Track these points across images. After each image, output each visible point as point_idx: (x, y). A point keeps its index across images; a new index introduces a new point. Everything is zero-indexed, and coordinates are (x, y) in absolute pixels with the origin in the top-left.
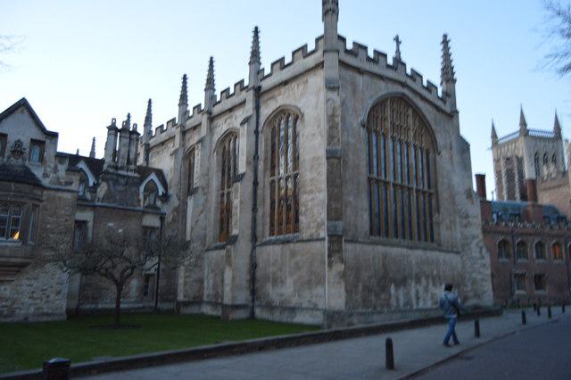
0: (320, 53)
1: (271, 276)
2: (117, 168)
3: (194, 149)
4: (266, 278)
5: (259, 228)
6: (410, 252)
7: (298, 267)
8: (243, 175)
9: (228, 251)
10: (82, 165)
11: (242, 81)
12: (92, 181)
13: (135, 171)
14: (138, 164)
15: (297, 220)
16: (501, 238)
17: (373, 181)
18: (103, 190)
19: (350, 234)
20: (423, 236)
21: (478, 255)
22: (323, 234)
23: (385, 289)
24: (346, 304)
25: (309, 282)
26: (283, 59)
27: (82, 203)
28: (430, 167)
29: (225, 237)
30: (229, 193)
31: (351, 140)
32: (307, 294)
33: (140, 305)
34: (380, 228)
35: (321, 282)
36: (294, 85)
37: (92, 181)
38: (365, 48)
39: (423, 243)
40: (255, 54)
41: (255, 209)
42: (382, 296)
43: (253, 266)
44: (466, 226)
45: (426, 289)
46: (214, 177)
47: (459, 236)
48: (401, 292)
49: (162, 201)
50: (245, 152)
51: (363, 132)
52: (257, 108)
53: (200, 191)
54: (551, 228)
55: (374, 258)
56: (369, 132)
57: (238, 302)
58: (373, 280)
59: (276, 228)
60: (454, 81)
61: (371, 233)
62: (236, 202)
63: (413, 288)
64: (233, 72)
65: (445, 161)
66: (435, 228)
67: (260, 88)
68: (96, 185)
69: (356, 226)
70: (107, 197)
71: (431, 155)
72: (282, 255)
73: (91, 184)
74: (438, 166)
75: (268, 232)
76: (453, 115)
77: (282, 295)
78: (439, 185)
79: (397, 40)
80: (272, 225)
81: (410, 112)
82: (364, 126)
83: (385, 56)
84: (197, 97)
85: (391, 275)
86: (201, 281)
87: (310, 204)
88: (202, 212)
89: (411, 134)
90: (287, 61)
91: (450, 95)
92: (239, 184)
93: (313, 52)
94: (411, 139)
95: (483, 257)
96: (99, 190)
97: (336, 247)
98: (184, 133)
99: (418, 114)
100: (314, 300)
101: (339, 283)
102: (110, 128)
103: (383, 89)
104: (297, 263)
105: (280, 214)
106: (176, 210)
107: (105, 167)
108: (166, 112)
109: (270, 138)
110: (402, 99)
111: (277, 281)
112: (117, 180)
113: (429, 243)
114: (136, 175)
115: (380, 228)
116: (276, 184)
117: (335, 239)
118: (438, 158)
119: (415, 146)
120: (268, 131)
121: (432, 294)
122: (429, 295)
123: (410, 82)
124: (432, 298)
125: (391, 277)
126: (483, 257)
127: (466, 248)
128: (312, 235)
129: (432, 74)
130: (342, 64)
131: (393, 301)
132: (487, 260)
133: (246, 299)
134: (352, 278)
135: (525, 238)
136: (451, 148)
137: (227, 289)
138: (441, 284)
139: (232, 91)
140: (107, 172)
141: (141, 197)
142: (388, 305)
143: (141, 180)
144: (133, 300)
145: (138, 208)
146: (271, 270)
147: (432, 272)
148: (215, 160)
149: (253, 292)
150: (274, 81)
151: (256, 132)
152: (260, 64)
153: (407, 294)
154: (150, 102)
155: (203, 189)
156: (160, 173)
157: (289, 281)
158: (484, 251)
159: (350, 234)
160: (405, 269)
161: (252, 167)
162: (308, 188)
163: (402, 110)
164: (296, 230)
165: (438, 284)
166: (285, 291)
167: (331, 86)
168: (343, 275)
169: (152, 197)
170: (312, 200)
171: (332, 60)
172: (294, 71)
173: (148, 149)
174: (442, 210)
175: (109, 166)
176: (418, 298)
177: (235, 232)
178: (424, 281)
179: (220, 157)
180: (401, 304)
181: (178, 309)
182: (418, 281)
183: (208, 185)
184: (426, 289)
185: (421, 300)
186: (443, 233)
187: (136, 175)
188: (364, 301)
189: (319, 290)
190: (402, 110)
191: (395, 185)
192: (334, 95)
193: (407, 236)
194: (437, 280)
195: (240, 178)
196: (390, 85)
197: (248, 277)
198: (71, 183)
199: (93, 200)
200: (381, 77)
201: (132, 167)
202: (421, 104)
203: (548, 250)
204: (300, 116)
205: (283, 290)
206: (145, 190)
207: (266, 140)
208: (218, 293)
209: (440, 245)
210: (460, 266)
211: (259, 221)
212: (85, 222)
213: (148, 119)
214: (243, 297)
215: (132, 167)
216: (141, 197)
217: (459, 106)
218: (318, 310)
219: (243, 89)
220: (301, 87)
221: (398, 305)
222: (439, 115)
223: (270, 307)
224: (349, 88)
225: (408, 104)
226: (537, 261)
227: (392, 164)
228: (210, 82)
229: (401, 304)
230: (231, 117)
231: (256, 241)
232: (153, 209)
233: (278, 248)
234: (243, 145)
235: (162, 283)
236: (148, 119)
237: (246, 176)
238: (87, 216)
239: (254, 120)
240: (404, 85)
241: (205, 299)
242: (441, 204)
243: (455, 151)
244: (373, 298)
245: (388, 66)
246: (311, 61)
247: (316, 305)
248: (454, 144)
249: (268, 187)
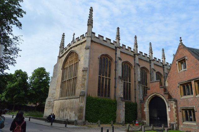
6: (66, 100)
138: (73, 111)
176: (66, 116)
178: (68, 110)
184: (68, 112)
185: (67, 116)
194: (72, 109)
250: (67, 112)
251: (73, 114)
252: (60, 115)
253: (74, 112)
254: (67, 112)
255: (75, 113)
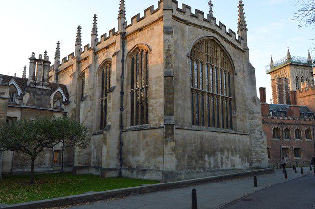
0: (161, 11)
1: (131, 150)
2: (35, 84)
3: (84, 72)
4: (128, 152)
5: (124, 121)
6: (217, 135)
7: (147, 145)
8: (114, 88)
9: (105, 135)
10: (12, 82)
11: (114, 29)
12: (19, 92)
13: (48, 86)
14: (50, 82)
15: (147, 115)
16: (275, 126)
17: (195, 91)
18: (26, 97)
19: (180, 124)
20: (225, 125)
21: (260, 137)
22: (162, 124)
23: (201, 157)
24: (177, 166)
25: (154, 154)
26: (138, 15)
27: (11, 106)
28: (231, 83)
29: (103, 126)
30: (106, 99)
31: (180, 65)
32: (153, 161)
33: (52, 169)
34: (198, 120)
35: (162, 153)
36: (145, 31)
37: (19, 92)
38: (190, 8)
39: (226, 130)
40: (122, 13)
41: (121, 109)
42: (200, 162)
43: (121, 144)
44: (252, 119)
45: (228, 158)
46: (97, 90)
47: (248, 125)
48: (212, 160)
49: (65, 105)
50: (115, 74)
51: (188, 60)
52: (123, 46)
53: (88, 98)
54: (305, 120)
55: (195, 138)
56: (191, 59)
57: (111, 167)
58: (194, 152)
59: (135, 120)
60: (246, 30)
61: (193, 123)
62: (109, 105)
63: (219, 156)
64: (108, 24)
65: (240, 79)
66: (233, 119)
67: (124, 33)
68: (22, 95)
69: (183, 119)
70: (29, 102)
71: (231, 76)
72: (138, 136)
73: (19, 94)
74: (235, 82)
75: (130, 123)
76: (245, 51)
77: (138, 162)
78: (236, 94)
79: (210, 4)
80: (132, 118)
81: (218, 49)
82: (188, 57)
83: (202, 13)
84: (86, 40)
85: (206, 149)
86: (89, 154)
87: (155, 105)
88: (89, 112)
89: (219, 62)
90: (141, 16)
91: (243, 38)
92: (111, 93)
93: (157, 10)
94: (219, 66)
95: (263, 138)
96: (24, 98)
97: (170, 132)
98: (79, 62)
99: (223, 49)
100: (157, 164)
101: (172, 154)
102: (31, 59)
103: (202, 34)
104: (147, 142)
105: (137, 112)
106: (74, 110)
107: (28, 83)
108: (68, 49)
109: (131, 65)
110: (213, 41)
111: (135, 153)
112: (36, 92)
113: (230, 130)
114: (48, 88)
115: (198, 120)
116: (135, 93)
117: (169, 128)
118: (235, 77)
119: (221, 70)
120: (129, 61)
121: (231, 160)
122: (230, 161)
123: (218, 30)
124: (231, 163)
125: (204, 150)
126: (263, 138)
127: (252, 132)
128: (156, 125)
129: (232, 25)
130: (175, 17)
131: (207, 165)
132: (265, 140)
133: (116, 165)
134: (180, 151)
135: (289, 126)
136: (244, 71)
137: (104, 158)
139: (108, 36)
140: (29, 87)
141: (52, 102)
142: (204, 168)
143: (51, 92)
144: (46, 166)
145: (50, 109)
146: (131, 146)
147: (231, 147)
148: (98, 80)
149: (121, 160)
150: (133, 29)
151: (122, 61)
152: (125, 18)
153: (215, 161)
154: (58, 43)
155: (90, 97)
156: (64, 88)
157: (142, 153)
158: (263, 133)
159: (180, 124)
160: (214, 146)
161: (119, 83)
162: (154, 96)
163: (213, 47)
164: (147, 122)
165: (235, 155)
166: (140, 159)
167: (168, 31)
168: (174, 149)
169: (59, 103)
170: (156, 103)
171: (169, 14)
172: (143, 23)
173: (57, 73)
174: (237, 109)
175: (31, 83)
176: (222, 163)
177: (109, 123)
178: (226, 153)
179: (101, 77)
180: (212, 166)
181: (75, 171)
182: (222, 152)
183: (93, 94)
184: (228, 158)
186: (238, 123)
187: (48, 88)
188: (188, 164)
189: (160, 159)
190: (213, 47)
191: (208, 94)
192: (168, 37)
193: (216, 124)
194: (234, 152)
195: (112, 90)
196: (205, 32)
197: (117, 151)
198: (4, 93)
199: (20, 105)
200: (200, 27)
201: (46, 83)
202: (225, 44)
203: (303, 134)
204: (149, 51)
205: (138, 159)
206: (54, 98)
207: (129, 66)
208: (99, 161)
209: (236, 130)
210: (248, 143)
211: (124, 117)
212: (16, 118)
213: (57, 54)
214: (114, 163)
215: (46, 83)
216: (52, 102)
217: (248, 46)
218: (160, 171)
219: (115, 34)
220: (149, 33)
221: (210, 168)
222: (236, 51)
223: (131, 169)
224: (180, 34)
225: (218, 44)
226: (296, 140)
227: (207, 80)
228: (95, 30)
229: (212, 166)
230: (107, 52)
231: (122, 128)
232: (59, 110)
233: (135, 133)
234: (114, 68)
235: (66, 155)
236: (57, 54)
237: (116, 89)
238: (16, 114)
239: (121, 53)
240: (214, 32)
241: (92, 165)
242: (237, 105)
243: (246, 74)
244: (194, 163)
245: (205, 20)
246: (155, 16)
247: (158, 168)
248: (245, 68)
249: (130, 95)
250: (224, 157)
251: (237, 159)
252: (207, 164)
253: (238, 155)
254: (224, 157)
255: (240, 157)
